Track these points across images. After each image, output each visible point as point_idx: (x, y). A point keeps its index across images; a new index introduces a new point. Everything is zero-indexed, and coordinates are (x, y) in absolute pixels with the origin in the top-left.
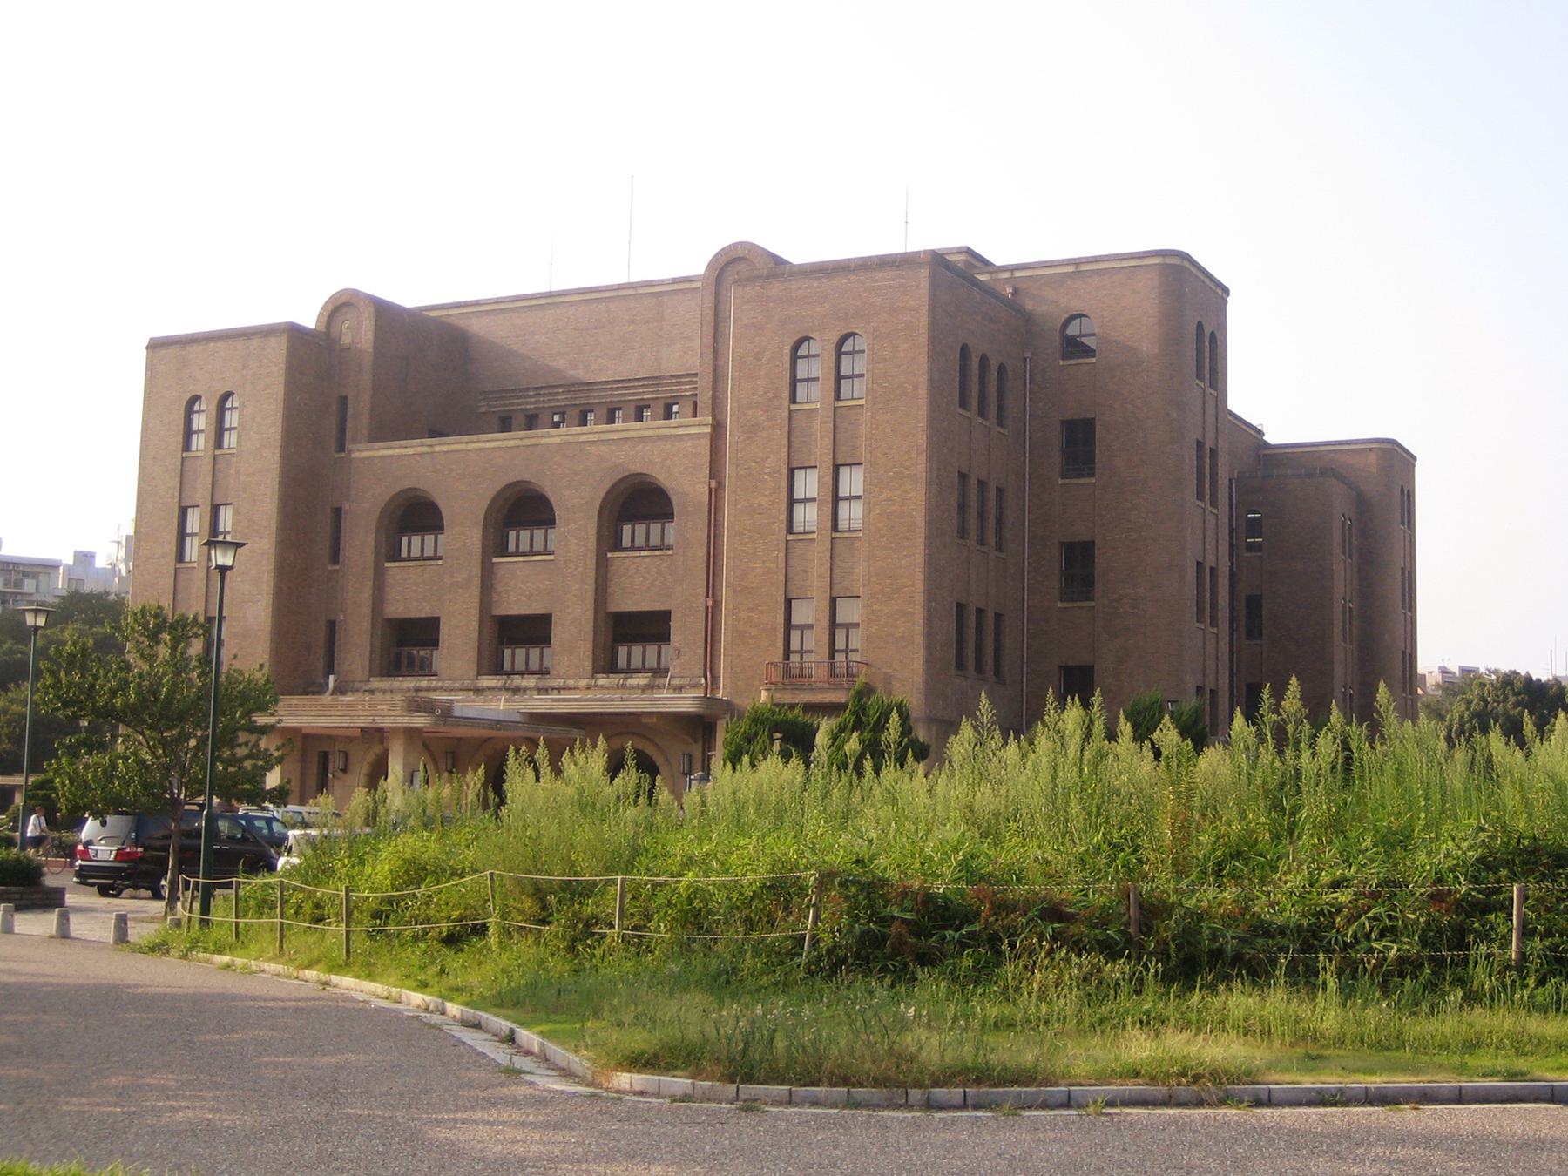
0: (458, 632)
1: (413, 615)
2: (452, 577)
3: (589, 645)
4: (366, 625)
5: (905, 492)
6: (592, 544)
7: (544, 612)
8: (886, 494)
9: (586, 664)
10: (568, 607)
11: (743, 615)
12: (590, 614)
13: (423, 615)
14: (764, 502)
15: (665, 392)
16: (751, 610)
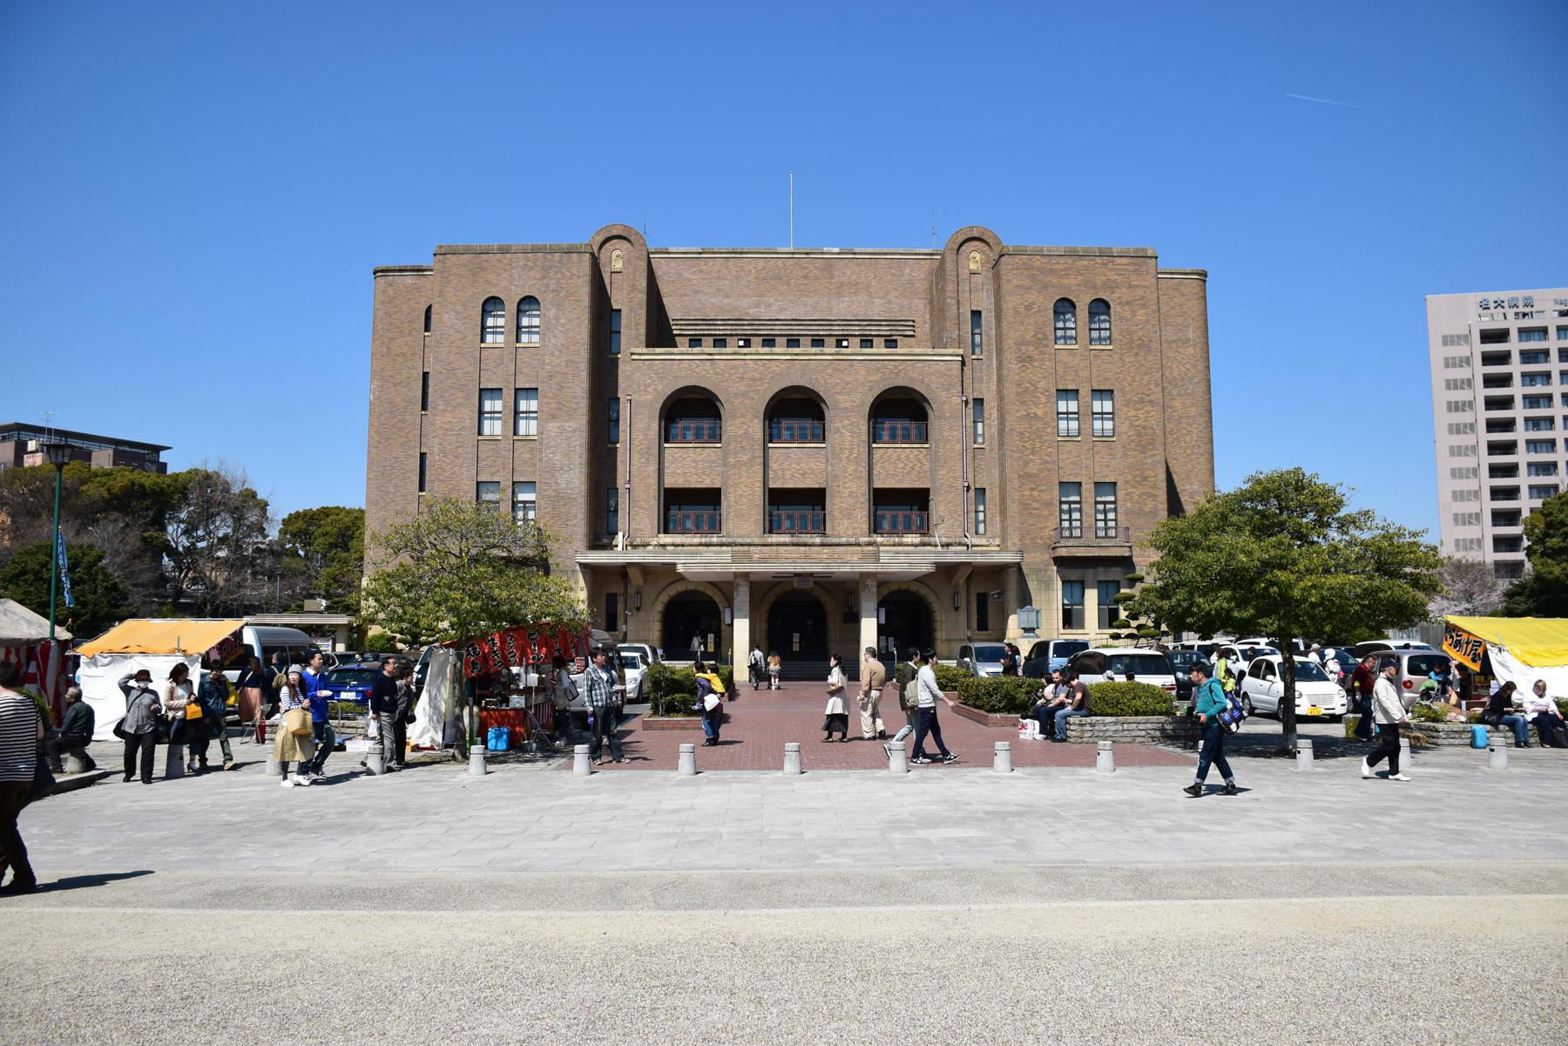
0: (745, 500)
1: (693, 486)
2: (736, 454)
3: (865, 513)
4: (653, 492)
5: (1148, 412)
6: (865, 437)
7: (817, 486)
8: (1133, 413)
9: (864, 526)
10: (845, 483)
11: (1027, 493)
12: (865, 488)
13: (704, 486)
14: (1039, 412)
15: (837, 331)
16: (1033, 489)
